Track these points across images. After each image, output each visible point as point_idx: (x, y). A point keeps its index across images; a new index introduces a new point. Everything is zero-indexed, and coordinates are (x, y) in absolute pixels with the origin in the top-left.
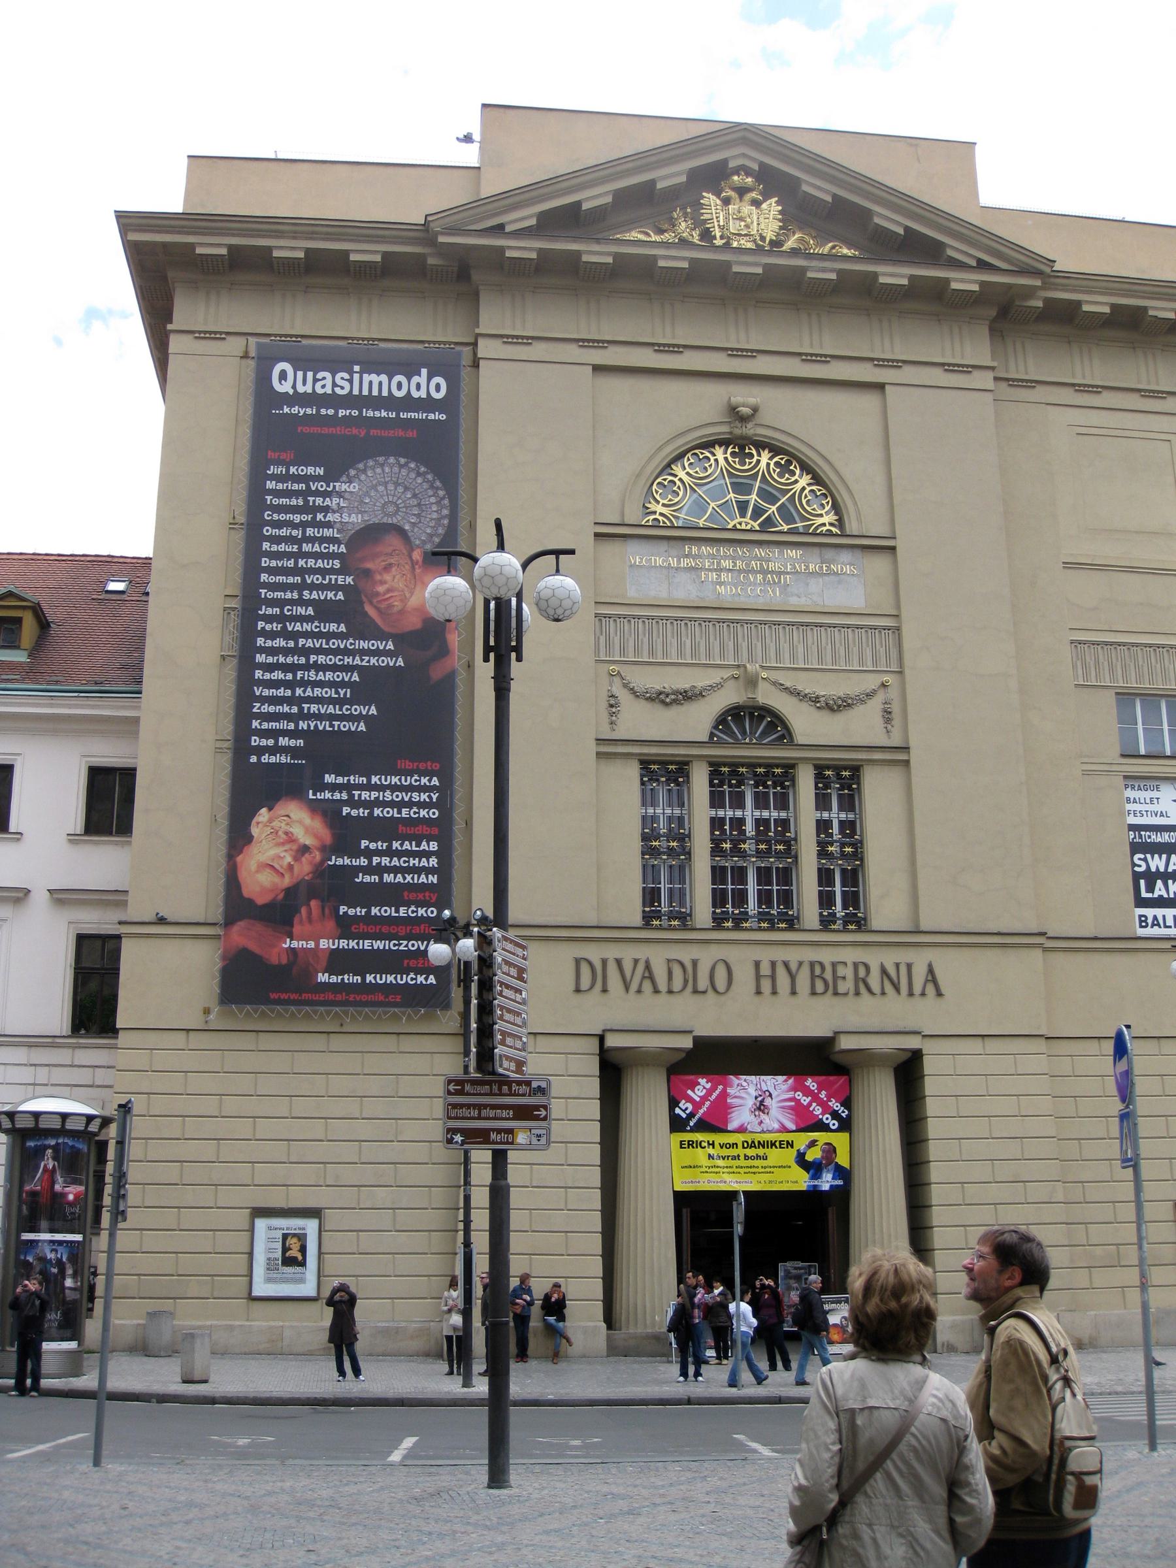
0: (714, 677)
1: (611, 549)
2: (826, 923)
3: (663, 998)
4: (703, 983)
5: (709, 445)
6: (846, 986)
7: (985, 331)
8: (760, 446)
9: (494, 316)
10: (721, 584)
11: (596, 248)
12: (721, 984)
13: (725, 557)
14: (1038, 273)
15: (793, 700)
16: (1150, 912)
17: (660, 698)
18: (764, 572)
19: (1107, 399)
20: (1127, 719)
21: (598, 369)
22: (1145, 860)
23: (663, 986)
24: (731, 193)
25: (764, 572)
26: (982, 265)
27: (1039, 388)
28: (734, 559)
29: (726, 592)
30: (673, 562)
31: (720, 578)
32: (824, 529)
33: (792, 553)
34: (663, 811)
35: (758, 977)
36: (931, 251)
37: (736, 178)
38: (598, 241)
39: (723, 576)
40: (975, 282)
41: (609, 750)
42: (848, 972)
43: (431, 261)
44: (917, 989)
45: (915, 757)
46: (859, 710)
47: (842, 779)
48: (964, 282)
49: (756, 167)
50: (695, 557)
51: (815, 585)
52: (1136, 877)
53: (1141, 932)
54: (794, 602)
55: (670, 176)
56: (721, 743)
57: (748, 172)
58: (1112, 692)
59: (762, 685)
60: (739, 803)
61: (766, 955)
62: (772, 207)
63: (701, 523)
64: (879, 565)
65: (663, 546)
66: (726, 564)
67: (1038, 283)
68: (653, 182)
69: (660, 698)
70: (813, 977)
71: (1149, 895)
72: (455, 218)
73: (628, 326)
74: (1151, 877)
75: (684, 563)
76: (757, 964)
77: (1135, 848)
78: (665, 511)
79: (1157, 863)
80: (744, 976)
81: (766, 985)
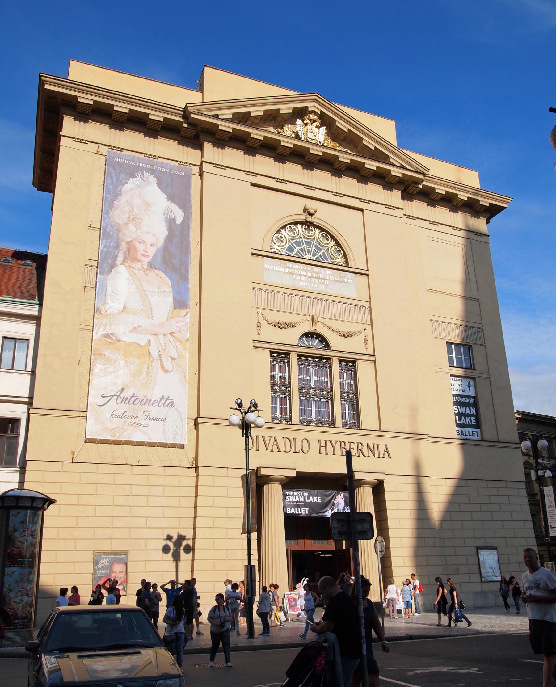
2: (344, 426)
3: (282, 453)
4: (298, 449)
5: (295, 224)
8: (316, 227)
10: (302, 281)
12: (305, 450)
13: (304, 270)
14: (423, 174)
15: (331, 332)
17: (279, 326)
18: (318, 278)
19: (440, 228)
21: (253, 185)
22: (458, 408)
23: (282, 450)
24: (309, 121)
25: (318, 278)
26: (402, 167)
28: (307, 271)
29: (303, 284)
30: (283, 270)
31: (301, 277)
32: (340, 264)
33: (328, 271)
34: (278, 374)
35: (320, 447)
36: (384, 158)
37: (311, 115)
39: (303, 278)
40: (400, 173)
44: (381, 456)
46: (355, 338)
47: (349, 364)
48: (397, 172)
49: (319, 112)
50: (291, 268)
63: (293, 255)
66: (304, 273)
67: (422, 177)
68: (279, 110)
69: (279, 326)
70: (341, 448)
71: (460, 422)
75: (287, 270)
76: (319, 441)
78: (279, 248)
80: (314, 446)
81: (323, 450)
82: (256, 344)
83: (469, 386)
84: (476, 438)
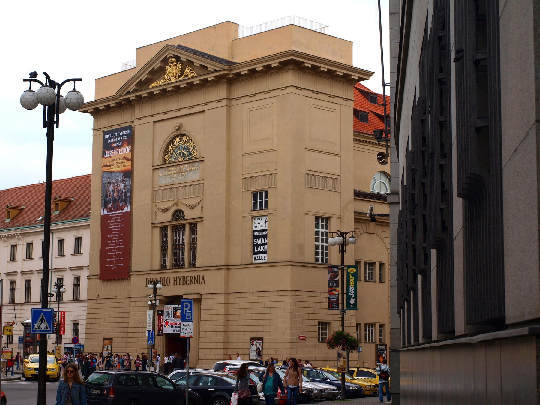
0: (171, 204)
1: (156, 172)
6: (189, 282)
7: (225, 86)
8: (184, 135)
9: (138, 112)
11: (144, 92)
16: (256, 256)
20: (255, 198)
21: (154, 122)
24: (171, 64)
26: (216, 71)
27: (242, 99)
33: (187, 166)
38: (143, 90)
41: (154, 225)
42: (189, 278)
43: (123, 103)
45: (204, 219)
46: (197, 207)
47: (193, 227)
49: (172, 56)
51: (191, 173)
52: (254, 246)
53: (254, 262)
54: (187, 180)
55: (157, 65)
56: (177, 220)
57: (173, 58)
58: (250, 192)
59: (180, 204)
60: (179, 236)
61: (176, 275)
62: (179, 65)
64: (201, 164)
65: (165, 169)
66: (175, 171)
67: (225, 72)
72: (120, 93)
73: (160, 107)
74: (258, 245)
77: (254, 237)
79: (259, 241)
81: (175, 282)
82: (153, 226)
83: (266, 222)
84: (266, 261)
